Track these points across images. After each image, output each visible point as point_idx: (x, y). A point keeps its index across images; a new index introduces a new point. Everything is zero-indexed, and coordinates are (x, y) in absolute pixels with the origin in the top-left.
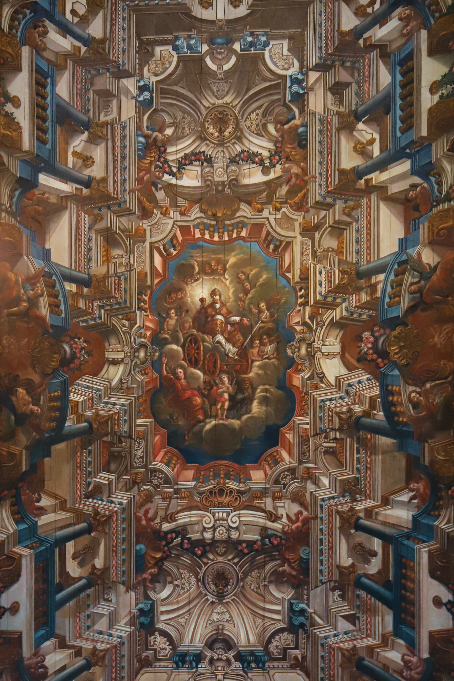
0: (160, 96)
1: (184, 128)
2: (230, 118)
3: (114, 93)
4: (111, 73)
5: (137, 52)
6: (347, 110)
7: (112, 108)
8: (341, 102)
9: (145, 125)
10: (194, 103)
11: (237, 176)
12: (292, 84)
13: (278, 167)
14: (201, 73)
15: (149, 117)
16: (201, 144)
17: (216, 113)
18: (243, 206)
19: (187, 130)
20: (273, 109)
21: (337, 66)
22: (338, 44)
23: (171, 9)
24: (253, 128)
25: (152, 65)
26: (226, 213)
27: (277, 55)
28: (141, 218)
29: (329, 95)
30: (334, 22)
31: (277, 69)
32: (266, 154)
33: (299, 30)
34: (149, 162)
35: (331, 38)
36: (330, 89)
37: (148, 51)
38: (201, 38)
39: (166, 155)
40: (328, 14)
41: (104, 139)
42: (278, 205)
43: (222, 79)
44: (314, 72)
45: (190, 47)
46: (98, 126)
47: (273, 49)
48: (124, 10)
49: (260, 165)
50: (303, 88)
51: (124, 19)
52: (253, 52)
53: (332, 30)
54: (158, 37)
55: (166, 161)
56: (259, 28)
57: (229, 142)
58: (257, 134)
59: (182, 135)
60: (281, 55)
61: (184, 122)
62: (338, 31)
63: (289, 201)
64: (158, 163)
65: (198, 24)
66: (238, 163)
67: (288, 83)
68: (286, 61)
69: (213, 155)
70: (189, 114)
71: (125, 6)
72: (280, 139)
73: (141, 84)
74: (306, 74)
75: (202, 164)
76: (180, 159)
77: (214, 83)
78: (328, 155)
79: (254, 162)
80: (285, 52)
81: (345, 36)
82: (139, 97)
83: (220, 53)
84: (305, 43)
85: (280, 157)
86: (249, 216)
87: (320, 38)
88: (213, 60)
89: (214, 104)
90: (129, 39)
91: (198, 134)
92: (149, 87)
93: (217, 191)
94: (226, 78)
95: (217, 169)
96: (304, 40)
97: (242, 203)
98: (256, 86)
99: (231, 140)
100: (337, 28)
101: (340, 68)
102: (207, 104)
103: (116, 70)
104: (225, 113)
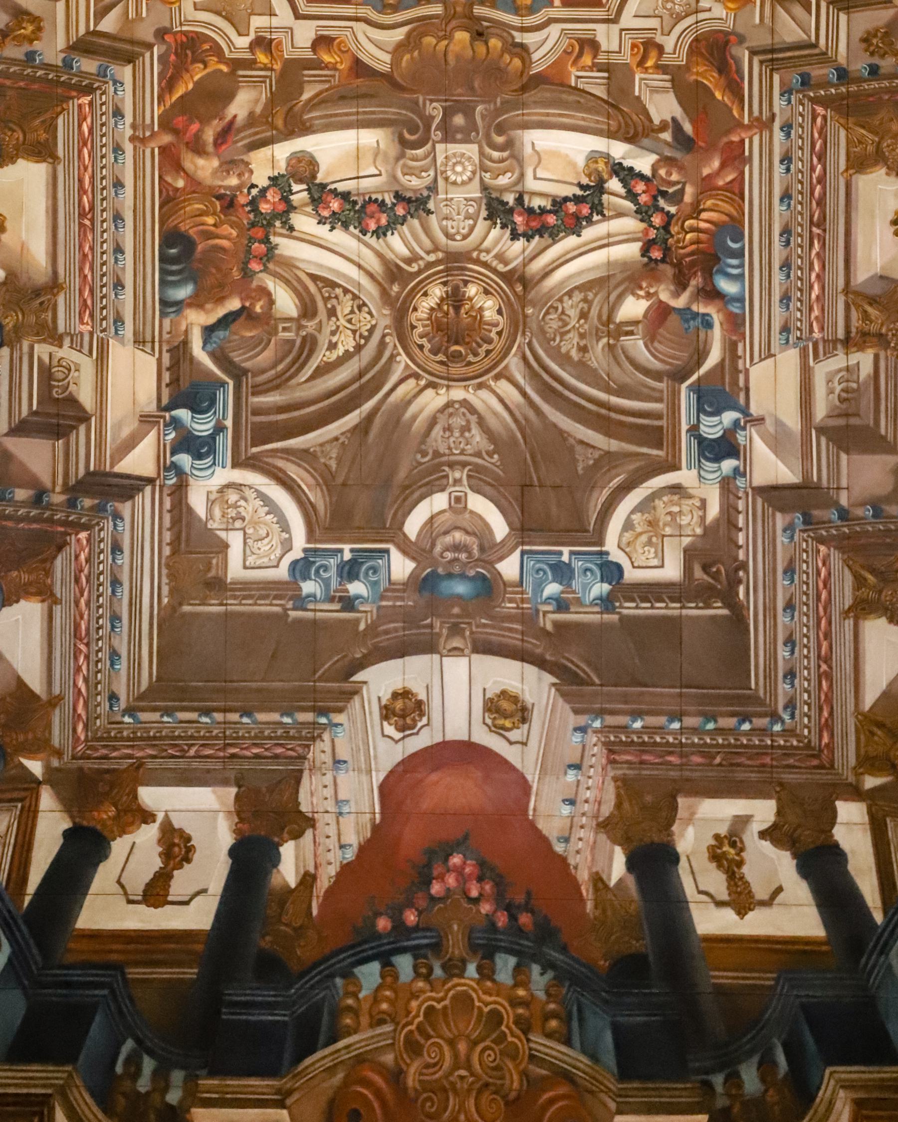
0: (663, 423)
1: (584, 315)
2: (424, 341)
3: (823, 440)
4: (836, 504)
5: (744, 566)
6: (25, 348)
7: (831, 391)
8: (47, 374)
9: (717, 333)
10: (548, 392)
11: (402, 156)
12: (213, 437)
13: (261, 179)
14: (525, 486)
15: (701, 355)
16: (525, 264)
17: (471, 358)
18: (381, 60)
19: (572, 310)
20: (274, 366)
21: (58, 489)
22: (55, 557)
23: (625, 698)
24: (346, 306)
25: (693, 528)
26: (440, 39)
27: (263, 532)
28: (732, 38)
29: (86, 397)
30: (69, 629)
31: (263, 489)
32: (304, 222)
33: (186, 608)
34: (704, 215)
35: (77, 580)
36: (84, 418)
37: (705, 568)
38: (523, 601)
39: (646, 232)
40: (87, 657)
41: (857, 293)
42: (262, 58)
43: (451, 465)
44: (137, 472)
45: (562, 572)
46: (880, 335)
47: (278, 552)
48: (791, 705)
49: (323, 186)
50: (175, 423)
51: (791, 674)
52: (347, 547)
53: (77, 603)
54: (673, 610)
55: (643, 214)
56: (325, 622)
57: (430, 265)
58: (334, 285)
59: (590, 296)
60: (250, 531)
61: (582, 336)
62: (57, 601)
63: (225, 68)
64: (673, 210)
65: (537, 646)
66: (397, 196)
67: (225, 443)
68: (232, 513)
69: (482, 225)
70: (564, 359)
71: (786, 717)
72: (255, 266)
73: (728, 465)
74: (166, 469)
75: (520, 200)
76: (596, 218)
77: (478, 454)
78: (92, 208)
79: (345, 196)
80: (235, 540)
81: (30, 584)
82: (736, 423)
83: (456, 548)
84: (168, 566)
85: (255, 210)
86: (359, 27)
87: (116, 582)
88: (483, 531)
89: (480, 386)
90: (770, 610)
91: (532, 295)
92: (701, 454)
93: (469, 113)
94: (437, 468)
95: (470, 179)
96: (172, 576)
97: (385, 68)
98: (336, 439)
99: (420, 272)
100: (57, 609)
101: (48, 484)
102: (504, 387)
103: (816, 513)
104: (441, 357)
